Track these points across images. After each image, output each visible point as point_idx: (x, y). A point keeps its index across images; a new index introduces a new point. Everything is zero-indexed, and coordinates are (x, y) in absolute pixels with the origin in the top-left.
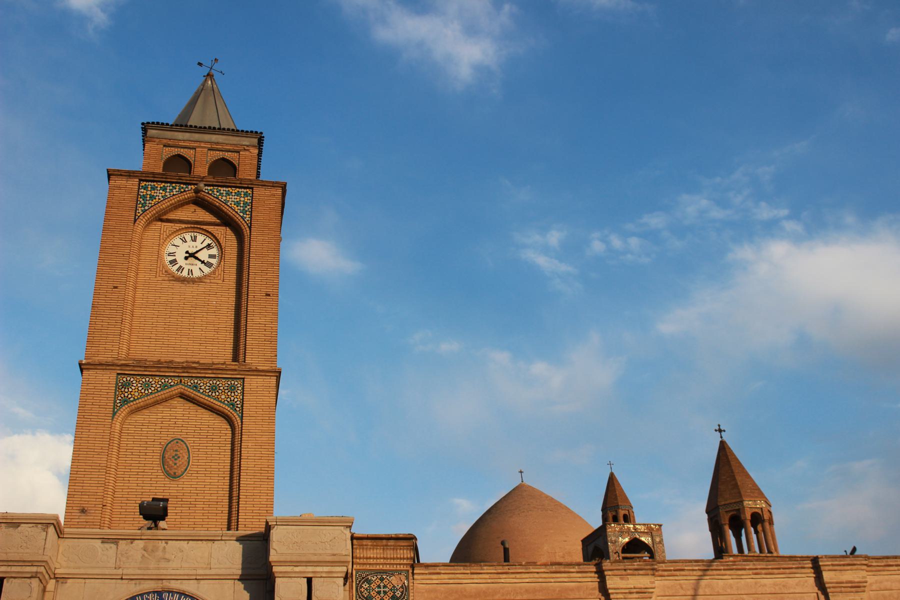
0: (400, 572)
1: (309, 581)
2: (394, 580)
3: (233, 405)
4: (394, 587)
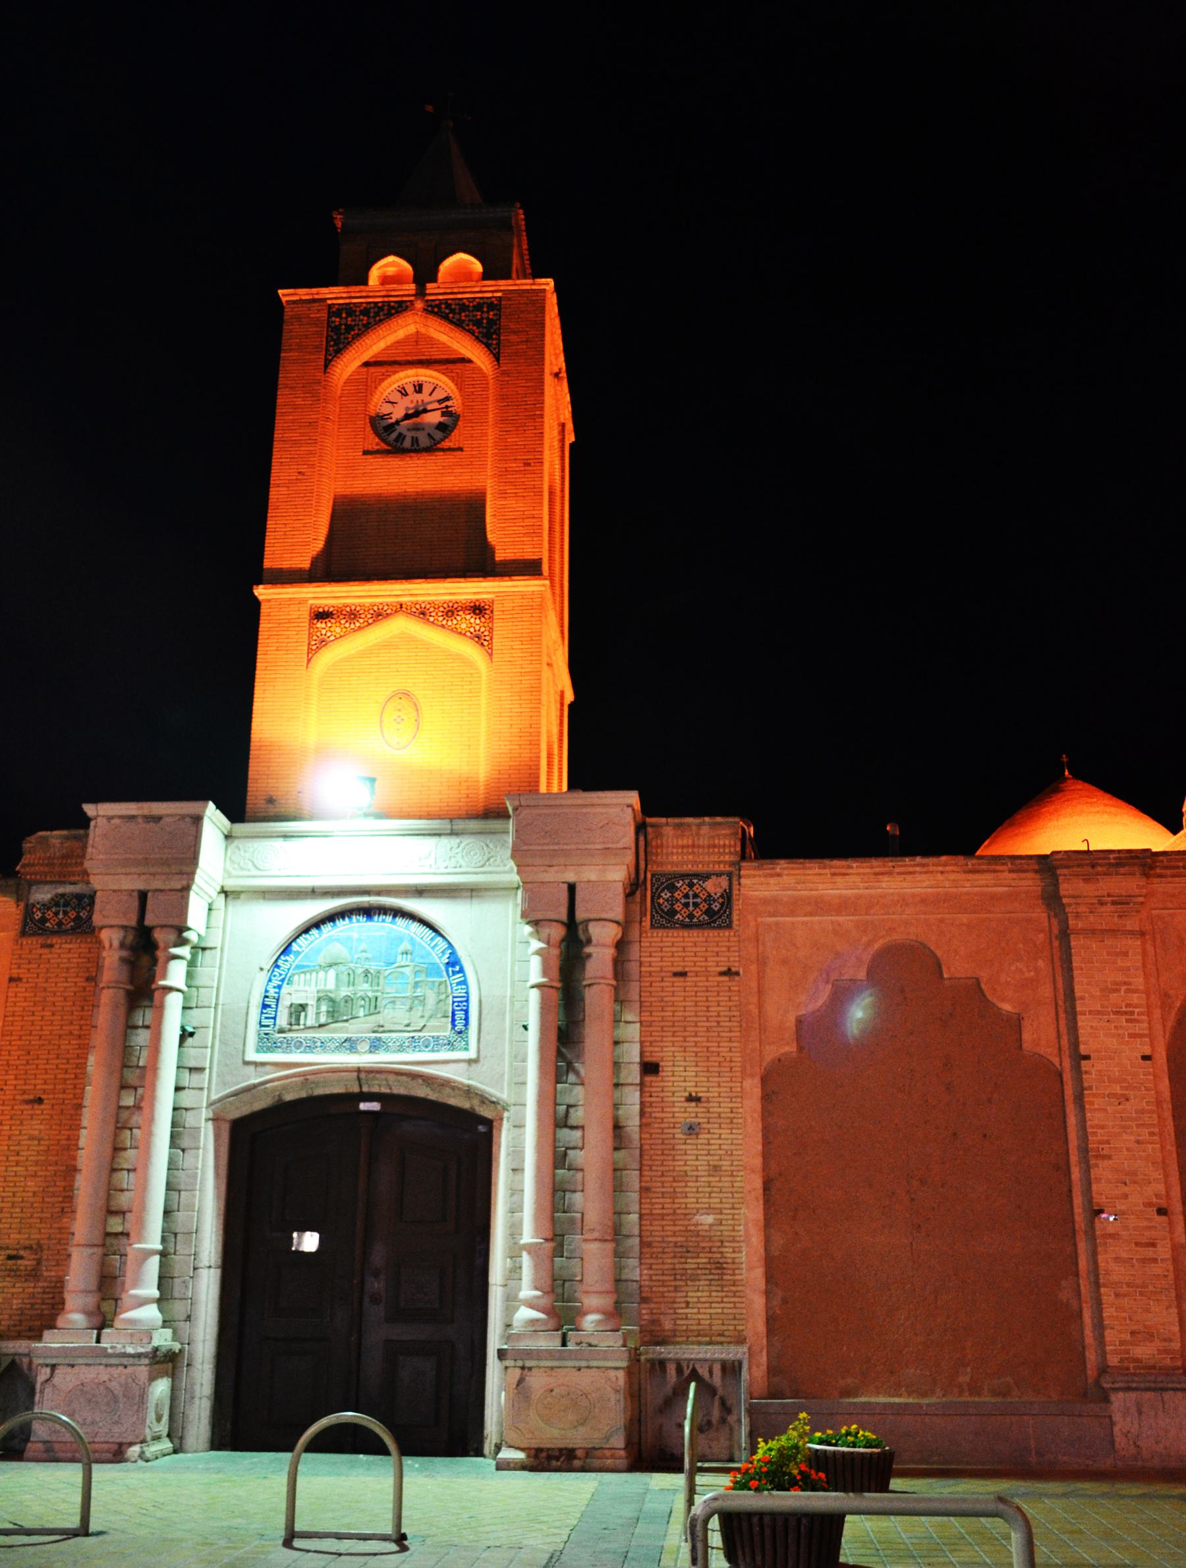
0: (719, 875)
1: (572, 888)
2: (710, 885)
3: (478, 638)
4: (710, 896)
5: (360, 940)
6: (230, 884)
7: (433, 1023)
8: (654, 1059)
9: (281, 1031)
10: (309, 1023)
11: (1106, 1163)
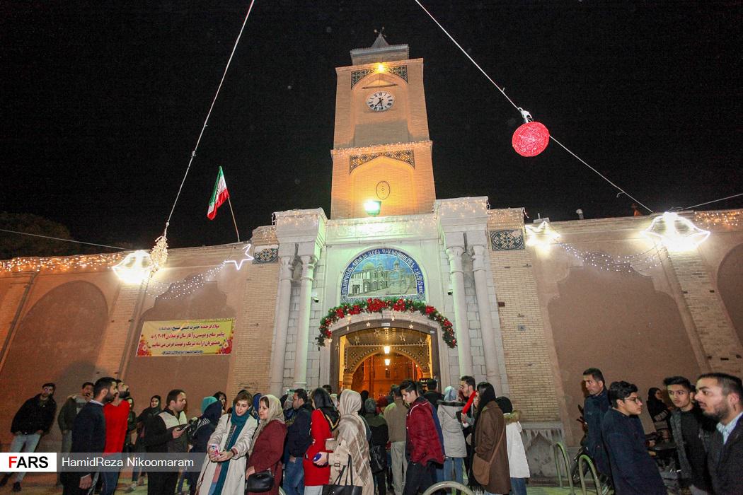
1: (465, 235)
3: (409, 162)
5: (378, 260)
6: (327, 242)
7: (410, 290)
8: (503, 301)
9: (350, 295)
10: (360, 292)
11: (706, 336)
